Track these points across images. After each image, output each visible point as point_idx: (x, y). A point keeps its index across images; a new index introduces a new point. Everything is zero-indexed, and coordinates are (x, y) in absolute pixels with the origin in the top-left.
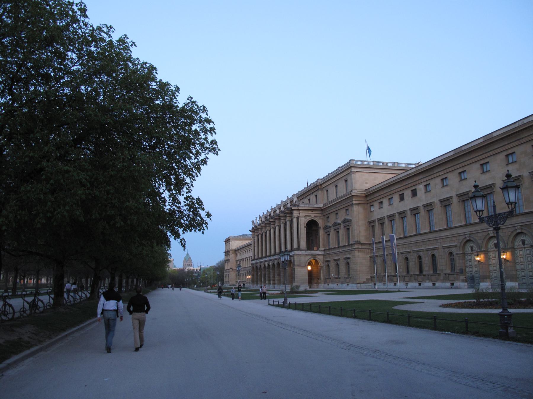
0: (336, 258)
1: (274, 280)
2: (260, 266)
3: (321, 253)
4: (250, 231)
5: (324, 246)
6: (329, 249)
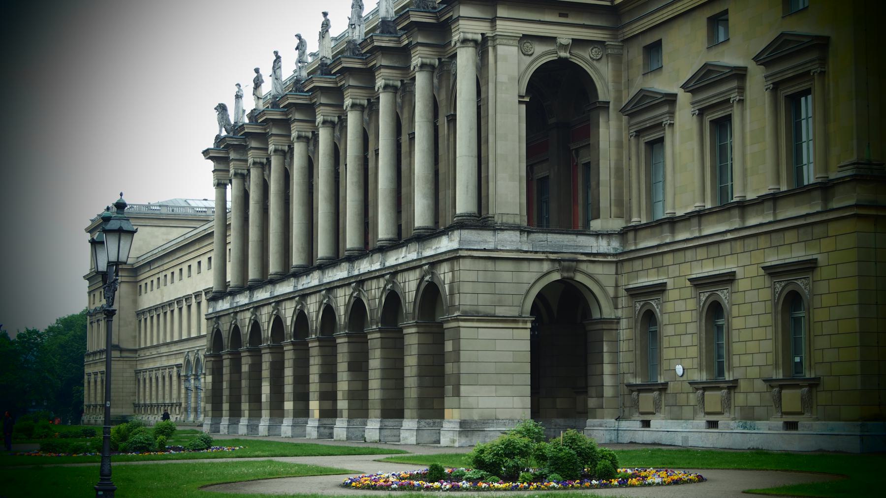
0: (708, 269)
1: (329, 396)
2: (256, 326)
3: (602, 246)
4: (206, 153)
5: (622, 207)
6: (655, 225)
